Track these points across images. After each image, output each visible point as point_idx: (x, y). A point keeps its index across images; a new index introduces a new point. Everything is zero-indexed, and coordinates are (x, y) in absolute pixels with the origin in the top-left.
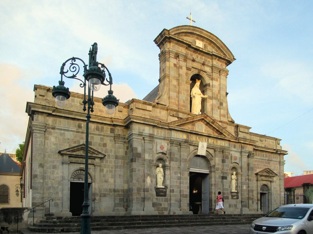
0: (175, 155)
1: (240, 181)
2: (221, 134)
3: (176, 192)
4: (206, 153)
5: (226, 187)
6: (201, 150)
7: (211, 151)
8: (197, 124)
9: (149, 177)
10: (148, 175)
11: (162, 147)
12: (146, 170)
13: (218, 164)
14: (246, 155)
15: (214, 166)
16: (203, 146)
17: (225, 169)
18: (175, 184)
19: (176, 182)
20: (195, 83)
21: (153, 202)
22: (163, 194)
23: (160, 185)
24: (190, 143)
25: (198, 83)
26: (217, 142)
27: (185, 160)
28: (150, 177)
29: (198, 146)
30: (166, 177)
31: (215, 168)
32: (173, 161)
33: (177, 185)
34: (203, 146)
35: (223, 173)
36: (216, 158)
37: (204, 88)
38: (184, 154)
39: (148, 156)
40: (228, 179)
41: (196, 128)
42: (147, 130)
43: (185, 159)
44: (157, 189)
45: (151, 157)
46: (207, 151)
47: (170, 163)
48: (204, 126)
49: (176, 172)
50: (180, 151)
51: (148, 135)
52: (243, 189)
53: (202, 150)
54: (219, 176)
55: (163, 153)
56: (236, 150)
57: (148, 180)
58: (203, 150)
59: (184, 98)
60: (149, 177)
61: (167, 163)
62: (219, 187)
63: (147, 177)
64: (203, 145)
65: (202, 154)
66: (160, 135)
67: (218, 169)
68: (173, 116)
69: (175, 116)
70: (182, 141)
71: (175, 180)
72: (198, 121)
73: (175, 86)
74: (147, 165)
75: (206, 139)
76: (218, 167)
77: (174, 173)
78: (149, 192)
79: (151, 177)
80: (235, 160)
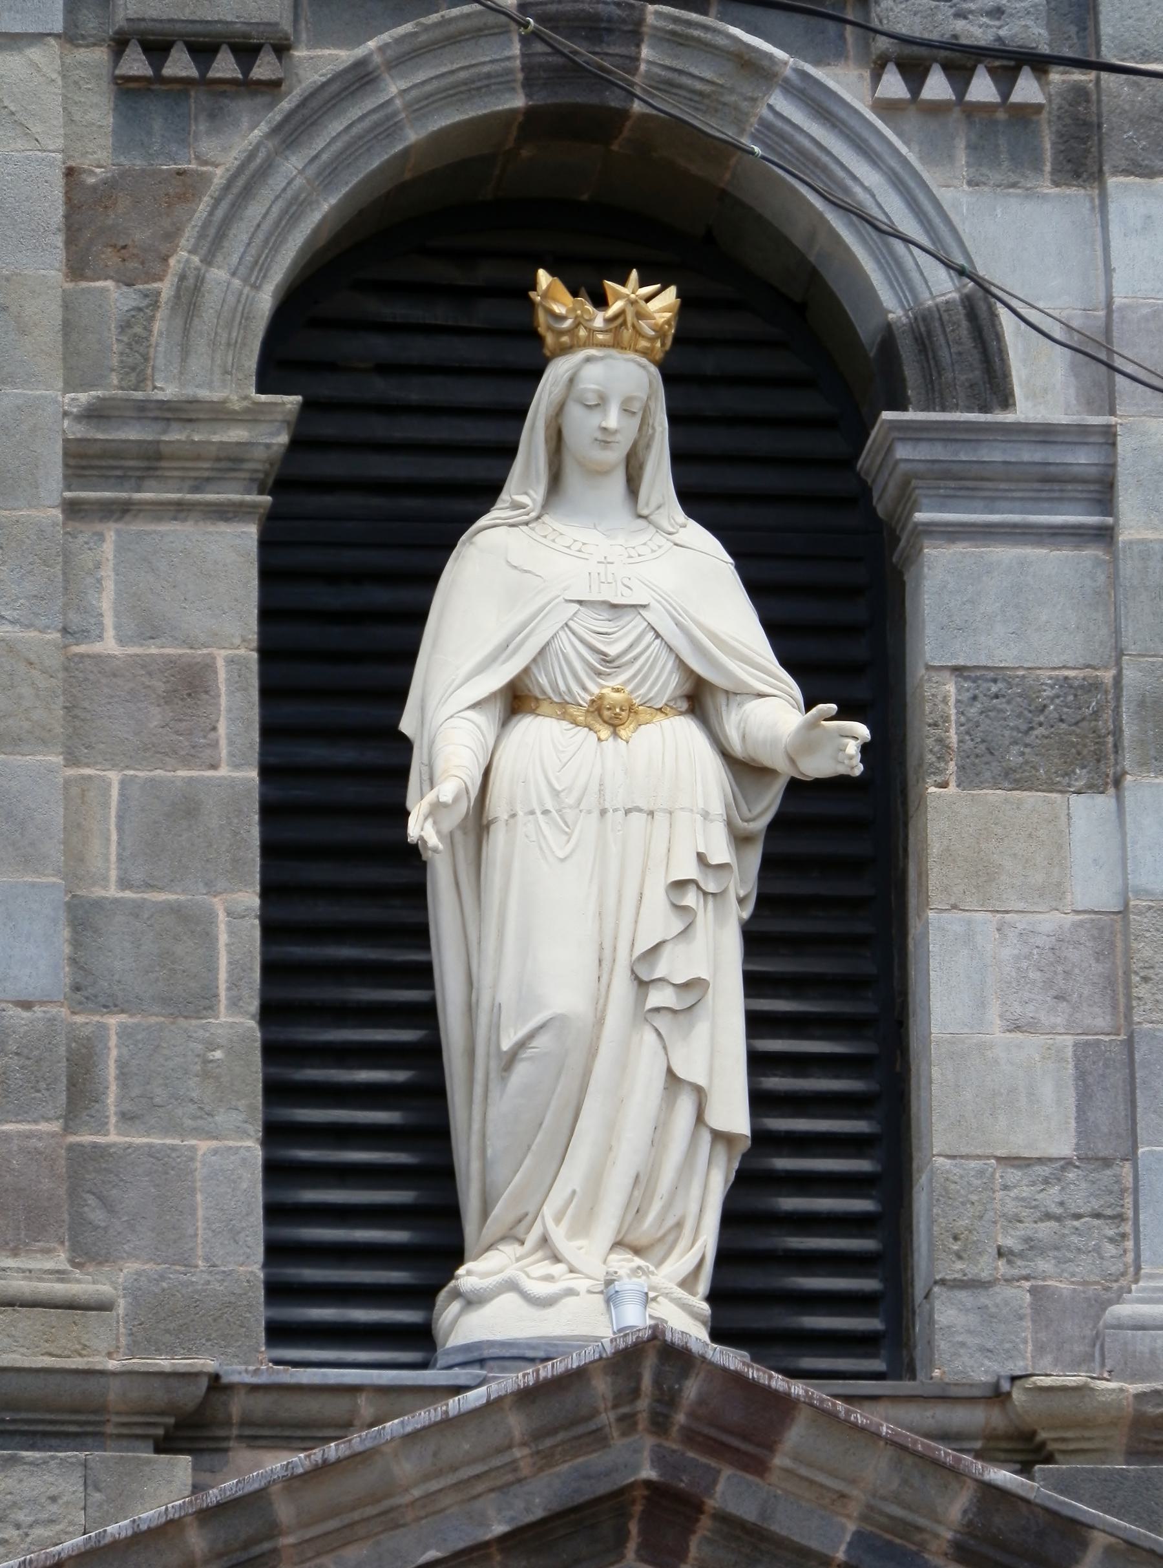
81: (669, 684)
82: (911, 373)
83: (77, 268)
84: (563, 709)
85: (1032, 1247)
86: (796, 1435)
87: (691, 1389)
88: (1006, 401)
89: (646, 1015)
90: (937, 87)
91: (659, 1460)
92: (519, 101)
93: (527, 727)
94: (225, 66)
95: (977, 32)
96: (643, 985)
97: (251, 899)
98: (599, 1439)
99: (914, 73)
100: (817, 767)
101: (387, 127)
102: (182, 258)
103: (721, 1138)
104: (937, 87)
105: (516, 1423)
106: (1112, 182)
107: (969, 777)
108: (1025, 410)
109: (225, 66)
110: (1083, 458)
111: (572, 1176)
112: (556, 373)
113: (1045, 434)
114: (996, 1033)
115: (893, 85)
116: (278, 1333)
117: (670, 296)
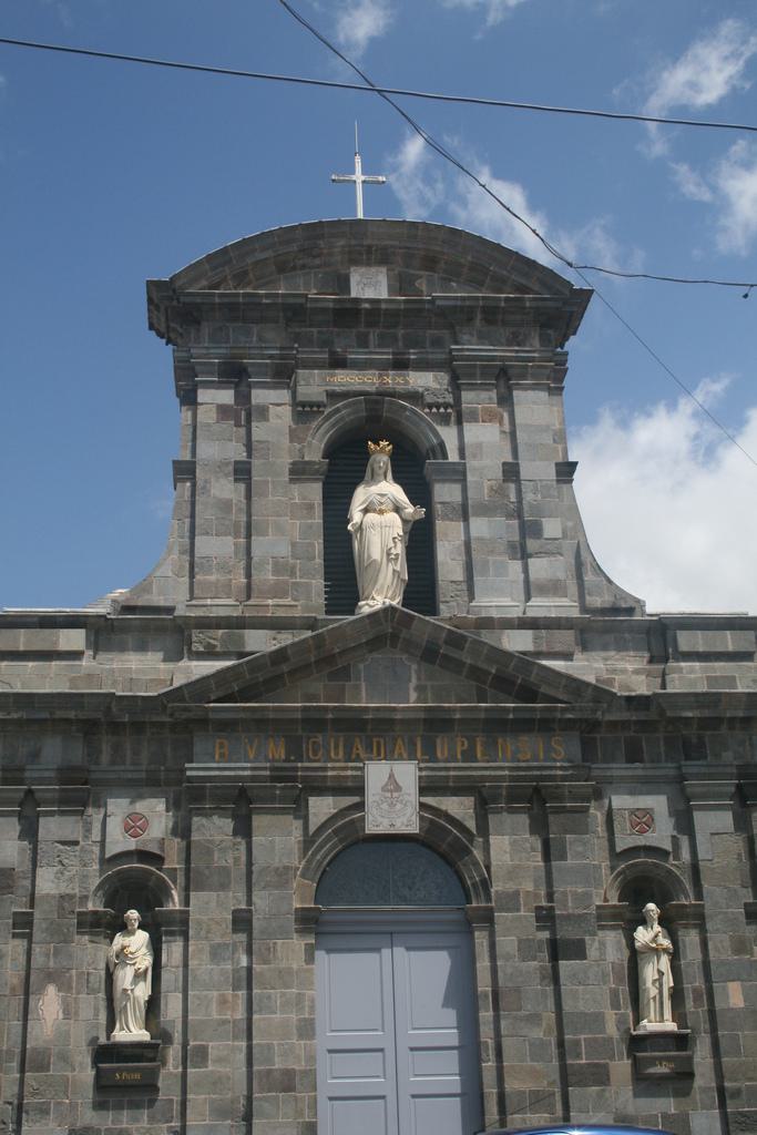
0: (216, 855)
1: (692, 954)
2: (529, 694)
3: (219, 1060)
4: (422, 818)
5: (581, 1007)
6: (385, 806)
7: (460, 808)
8: (361, 666)
9: (51, 990)
10: (51, 977)
11: (134, 825)
12: (38, 950)
13: (513, 873)
14: (720, 796)
15: (486, 884)
16: (393, 785)
17: (564, 894)
18: (215, 1016)
19: (223, 1001)
20: (368, 459)
21: (79, 1125)
22: (137, 1076)
23: (133, 1032)
24: (304, 779)
25: (381, 453)
26: (491, 746)
27: (282, 876)
28: (59, 991)
29: (359, 789)
30: (165, 976)
31: (489, 899)
32: (200, 888)
33: (225, 1022)
34: (393, 785)
35: (546, 917)
36: (493, 839)
37: (415, 470)
38: (272, 842)
39: (52, 877)
40: (592, 951)
41: (357, 688)
42: (54, 752)
43: (278, 869)
44: (106, 1053)
45: (71, 880)
46: (422, 806)
47: (187, 902)
48: (414, 667)
49: (219, 945)
50: (244, 830)
51: (52, 774)
52: (719, 1005)
53: (392, 805)
54: (520, 941)
55: (143, 855)
56: (640, 772)
57: (49, 1004)
58: (399, 806)
59: (283, 550)
60: (51, 990)
61: (175, 904)
62: (523, 1013)
63: (41, 990)
64: (391, 776)
65: (392, 825)
66: (133, 764)
67: (512, 902)
68: (210, 654)
69: (218, 649)
70: (253, 779)
71: (215, 993)
72: (371, 652)
73: (226, 506)
74: (44, 926)
75: (415, 745)
76: (511, 887)
77: (206, 957)
78: (49, 1071)
79: (64, 986)
80: (642, 832)
81: (391, 506)
82: (431, 455)
83: (291, 441)
84: (375, 511)
85: (457, 596)
86: (415, 622)
87: (397, 615)
88: (447, 458)
89: (389, 560)
90: (434, 410)
91: (393, 628)
92: (364, 414)
93: (369, 515)
94: (315, 409)
95: (441, 401)
96: (388, 554)
97: (321, 541)
98: (381, 624)
99: (430, 408)
100: (417, 518)
101: (342, 418)
102: (309, 439)
103: (403, 580)
104: (434, 410)
105: (367, 621)
106: (465, 424)
107: (443, 519)
108: (450, 460)
109: (315, 409)
110: (461, 468)
111: (378, 586)
112: (372, 457)
113: (454, 463)
114: (449, 561)
115: (427, 410)
116: (327, 613)
117: (391, 447)
